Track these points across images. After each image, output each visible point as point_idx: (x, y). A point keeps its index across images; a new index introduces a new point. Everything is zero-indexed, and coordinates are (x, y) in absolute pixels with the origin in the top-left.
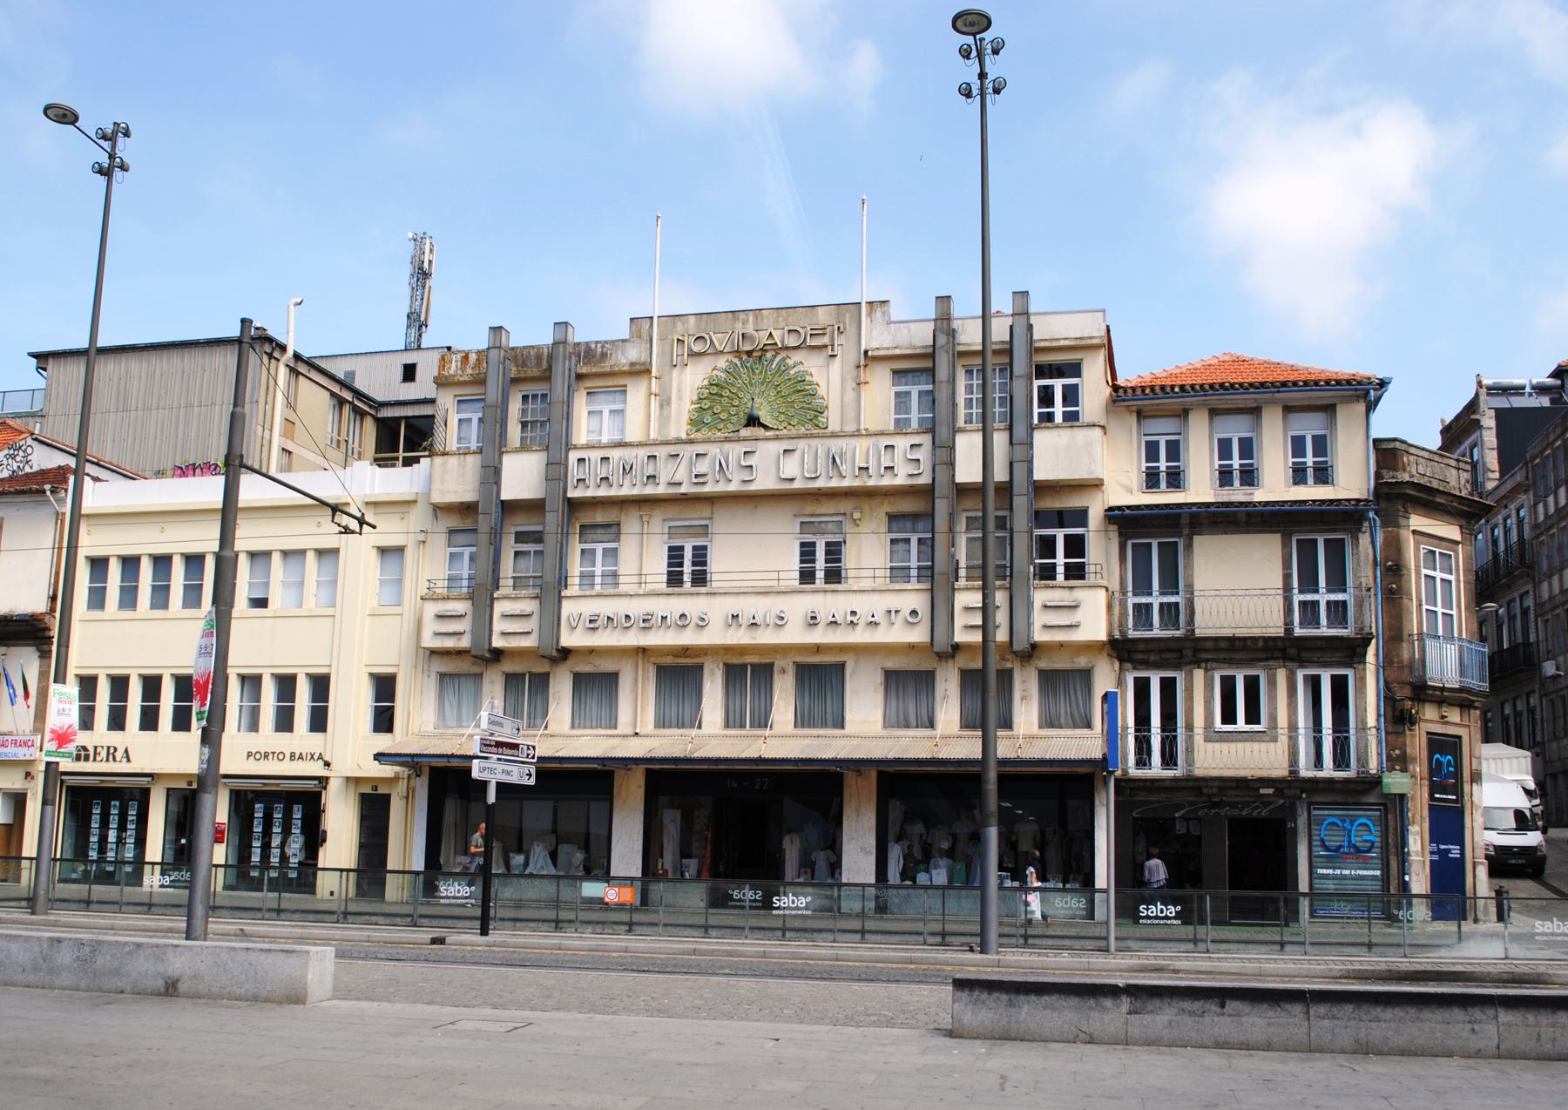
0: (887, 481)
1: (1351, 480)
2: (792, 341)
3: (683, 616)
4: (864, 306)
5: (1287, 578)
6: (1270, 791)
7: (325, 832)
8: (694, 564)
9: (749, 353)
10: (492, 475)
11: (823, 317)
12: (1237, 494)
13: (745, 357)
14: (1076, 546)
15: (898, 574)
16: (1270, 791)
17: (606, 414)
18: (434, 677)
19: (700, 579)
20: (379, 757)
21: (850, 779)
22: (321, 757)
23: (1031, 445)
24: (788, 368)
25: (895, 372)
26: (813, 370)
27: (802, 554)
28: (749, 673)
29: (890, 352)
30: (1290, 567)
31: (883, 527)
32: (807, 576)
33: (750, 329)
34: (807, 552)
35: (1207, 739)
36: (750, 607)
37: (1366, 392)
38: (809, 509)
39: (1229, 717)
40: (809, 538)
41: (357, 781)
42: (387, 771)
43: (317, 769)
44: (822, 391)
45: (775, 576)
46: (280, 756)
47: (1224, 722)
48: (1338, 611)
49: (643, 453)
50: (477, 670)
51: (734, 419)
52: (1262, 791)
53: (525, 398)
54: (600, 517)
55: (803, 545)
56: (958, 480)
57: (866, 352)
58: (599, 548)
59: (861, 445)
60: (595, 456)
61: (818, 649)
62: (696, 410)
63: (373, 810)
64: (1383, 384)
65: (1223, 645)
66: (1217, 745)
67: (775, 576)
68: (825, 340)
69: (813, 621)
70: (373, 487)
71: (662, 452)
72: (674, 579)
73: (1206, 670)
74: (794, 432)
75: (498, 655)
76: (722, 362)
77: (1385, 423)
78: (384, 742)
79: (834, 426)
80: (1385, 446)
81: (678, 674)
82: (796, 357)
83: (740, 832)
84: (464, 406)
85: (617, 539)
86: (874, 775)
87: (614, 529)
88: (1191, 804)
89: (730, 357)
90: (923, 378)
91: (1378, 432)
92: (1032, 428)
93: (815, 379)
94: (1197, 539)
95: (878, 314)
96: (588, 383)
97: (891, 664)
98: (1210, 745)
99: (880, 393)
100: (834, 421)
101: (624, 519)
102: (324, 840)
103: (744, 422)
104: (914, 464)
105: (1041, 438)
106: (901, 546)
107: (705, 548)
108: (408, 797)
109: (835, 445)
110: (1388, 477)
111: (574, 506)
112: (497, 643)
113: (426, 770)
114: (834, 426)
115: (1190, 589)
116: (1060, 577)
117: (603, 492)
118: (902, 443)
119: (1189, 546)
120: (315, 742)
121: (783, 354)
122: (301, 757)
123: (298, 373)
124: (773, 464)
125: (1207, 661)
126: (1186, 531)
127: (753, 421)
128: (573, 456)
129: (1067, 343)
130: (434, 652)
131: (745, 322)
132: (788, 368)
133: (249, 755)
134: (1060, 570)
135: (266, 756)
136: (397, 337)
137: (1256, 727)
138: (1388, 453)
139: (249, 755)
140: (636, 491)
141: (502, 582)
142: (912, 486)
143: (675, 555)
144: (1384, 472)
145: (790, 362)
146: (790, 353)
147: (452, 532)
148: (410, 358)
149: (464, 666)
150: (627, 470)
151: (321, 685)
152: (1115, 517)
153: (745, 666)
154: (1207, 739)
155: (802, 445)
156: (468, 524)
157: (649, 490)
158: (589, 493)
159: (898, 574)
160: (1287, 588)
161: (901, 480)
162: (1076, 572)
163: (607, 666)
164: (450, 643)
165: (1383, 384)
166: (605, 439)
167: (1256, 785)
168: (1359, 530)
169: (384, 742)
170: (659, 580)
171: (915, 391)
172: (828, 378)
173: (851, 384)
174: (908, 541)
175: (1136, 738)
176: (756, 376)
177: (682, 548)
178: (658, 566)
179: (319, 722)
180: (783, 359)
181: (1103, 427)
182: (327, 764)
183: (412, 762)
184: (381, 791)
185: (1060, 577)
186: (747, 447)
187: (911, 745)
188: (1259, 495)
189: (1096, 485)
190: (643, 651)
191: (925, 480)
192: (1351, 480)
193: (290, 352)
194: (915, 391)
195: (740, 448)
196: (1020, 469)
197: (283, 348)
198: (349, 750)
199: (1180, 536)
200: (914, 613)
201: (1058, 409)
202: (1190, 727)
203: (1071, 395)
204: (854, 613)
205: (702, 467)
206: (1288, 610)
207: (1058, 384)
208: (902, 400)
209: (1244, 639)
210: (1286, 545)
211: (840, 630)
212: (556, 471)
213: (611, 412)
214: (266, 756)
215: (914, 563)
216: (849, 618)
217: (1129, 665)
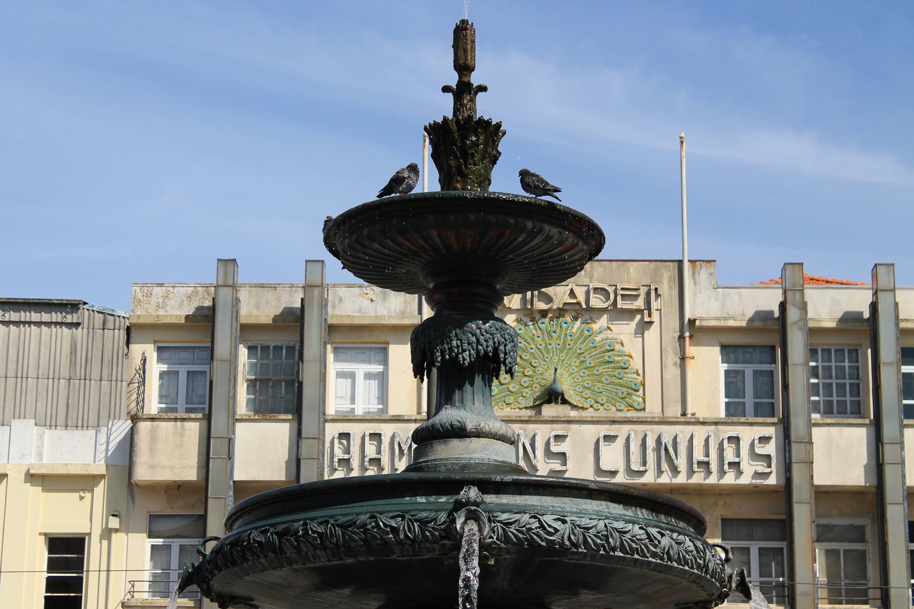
2: (597, 302)
4: (687, 266)
23: (902, 444)
26: (624, 338)
29: (722, 324)
56: (817, 481)
59: (700, 433)
60: (357, 430)
68: (640, 303)
70: (40, 455)
74: (602, 414)
84: (166, 355)
93: (627, 349)
96: (337, 338)
99: (709, 367)
109: (667, 433)
114: (653, 408)
142: (756, 486)
147: (153, 518)
155: (623, 431)
161: (746, 479)
166: (359, 412)
171: (749, 370)
172: (645, 350)
173: (672, 358)
186: (559, 429)
194: (749, 370)
196: (890, 473)
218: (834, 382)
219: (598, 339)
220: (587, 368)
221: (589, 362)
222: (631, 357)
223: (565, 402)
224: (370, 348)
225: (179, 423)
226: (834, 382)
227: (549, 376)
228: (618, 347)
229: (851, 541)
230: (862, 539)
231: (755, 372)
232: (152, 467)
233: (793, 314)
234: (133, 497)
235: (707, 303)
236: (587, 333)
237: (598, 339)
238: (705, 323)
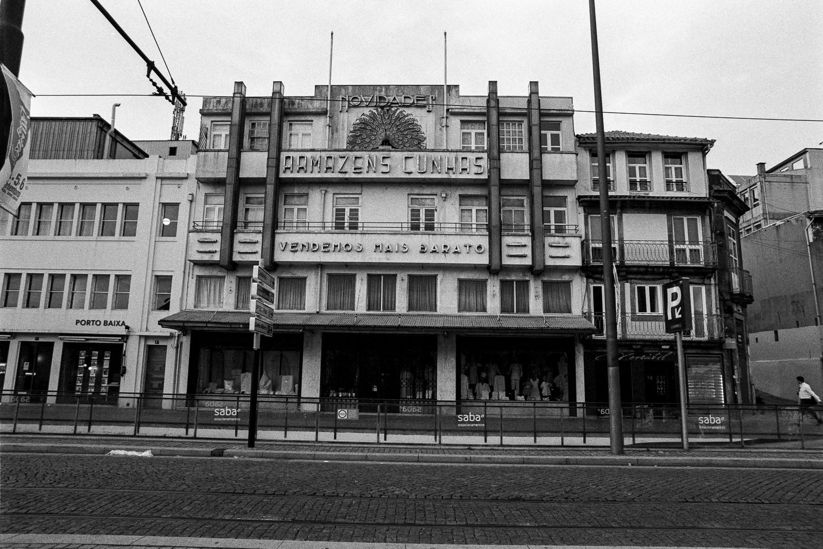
0: (464, 176)
1: (699, 189)
3: (347, 245)
5: (670, 236)
6: (667, 347)
7: (125, 368)
8: (351, 219)
9: (382, 108)
10: (236, 163)
11: (423, 92)
12: (639, 192)
13: (379, 110)
14: (560, 216)
15: (464, 227)
16: (667, 347)
17: (300, 136)
18: (195, 278)
19: (353, 226)
20: (162, 323)
21: (441, 339)
22: (123, 323)
24: (405, 116)
25: (462, 121)
27: (412, 215)
28: (381, 277)
30: (672, 232)
31: (457, 202)
32: (415, 227)
33: (383, 94)
34: (415, 214)
35: (633, 319)
36: (386, 240)
37: (702, 147)
38: (416, 191)
39: (643, 308)
40: (416, 207)
41: (147, 338)
42: (167, 332)
43: (122, 331)
44: (423, 130)
45: (400, 225)
46: (97, 323)
47: (640, 311)
48: (695, 252)
49: (324, 155)
50: (220, 274)
51: (373, 142)
52: (663, 347)
53: (253, 125)
54: (296, 191)
55: (412, 210)
56: (503, 177)
57: (448, 110)
58: (296, 208)
61: (423, 266)
62: (352, 136)
63: (154, 352)
64: (712, 142)
65: (642, 269)
66: (638, 323)
67: (400, 225)
69: (423, 250)
71: (334, 154)
72: (339, 226)
73: (631, 283)
75: (232, 266)
76: (367, 111)
77: (713, 161)
78: (164, 315)
79: (430, 146)
80: (713, 173)
81: (340, 278)
82: (408, 111)
83: (377, 366)
84: (218, 128)
85: (306, 203)
86: (454, 338)
87: (305, 198)
88: (625, 354)
89: (372, 109)
90: (477, 126)
91: (709, 167)
92: (542, 151)
93: (419, 123)
94: (624, 216)
95: (453, 92)
97: (463, 276)
98: (634, 322)
100: (429, 144)
101: (310, 192)
102: (124, 372)
103: (380, 143)
104: (479, 168)
105: (547, 158)
106: (466, 214)
107: (357, 210)
108: (179, 347)
110: (716, 188)
111: (281, 184)
112: (237, 258)
113: (189, 332)
115: (621, 240)
116: (553, 232)
117: (301, 175)
118: (472, 156)
119: (620, 220)
120: (119, 315)
121: (401, 109)
122: (111, 323)
123: (117, 141)
124: (400, 164)
125: (631, 279)
126: (619, 211)
127: (386, 142)
128: (284, 155)
129: (555, 112)
130: (197, 263)
131: (380, 91)
132: (405, 116)
133: (77, 322)
134: (553, 227)
135: (88, 323)
136: (167, 135)
137: (645, 314)
138: (715, 177)
139: (77, 322)
140: (319, 176)
141: (239, 224)
142: (475, 180)
143: (340, 213)
144: (713, 186)
145: (405, 114)
146: (405, 109)
148: (174, 144)
149: (216, 272)
150: (315, 163)
151: (124, 280)
152: (583, 202)
153: (380, 276)
154: (633, 319)
156: (219, 190)
157: (329, 175)
158: (292, 176)
159: (464, 227)
160: (670, 241)
162: (560, 230)
163: (300, 274)
164: (206, 257)
165: (712, 142)
167: (662, 343)
168: (705, 214)
169: (164, 315)
170: (329, 226)
171: (473, 132)
174: (471, 210)
175: (595, 318)
176: (386, 118)
177: (344, 210)
178: (330, 217)
179: (122, 303)
180: (401, 112)
181: (577, 155)
182: (127, 328)
183: (182, 325)
184: (161, 343)
185: (553, 232)
186: (385, 154)
187: (471, 319)
188: (651, 194)
189: (571, 185)
190: (320, 266)
191: (485, 176)
192: (699, 189)
193: (112, 130)
194: (473, 132)
195: (380, 155)
196: (536, 172)
197: (109, 126)
198: (139, 318)
199: (615, 214)
200: (479, 247)
201: (549, 147)
202: (623, 313)
203: (556, 140)
204: (445, 246)
205: (359, 163)
206: (671, 252)
207: (549, 133)
208: (465, 137)
209: (653, 267)
210: (669, 221)
211: (437, 255)
212: (275, 163)
213: (303, 134)
214: (88, 323)
215: (474, 221)
216: (443, 249)
217: (591, 280)
218: (511, 137)
219: (406, 118)
220: (401, 131)
221: (402, 129)
222: (420, 126)
223: (389, 145)
224: (307, 124)
225: (216, 153)
226: (511, 137)
227: (383, 134)
228: (415, 122)
229: (517, 206)
230: (523, 206)
231: (476, 134)
232: (204, 172)
233: (493, 103)
234: (199, 188)
235: (454, 102)
236: (401, 117)
237: (406, 118)
238: (453, 111)
